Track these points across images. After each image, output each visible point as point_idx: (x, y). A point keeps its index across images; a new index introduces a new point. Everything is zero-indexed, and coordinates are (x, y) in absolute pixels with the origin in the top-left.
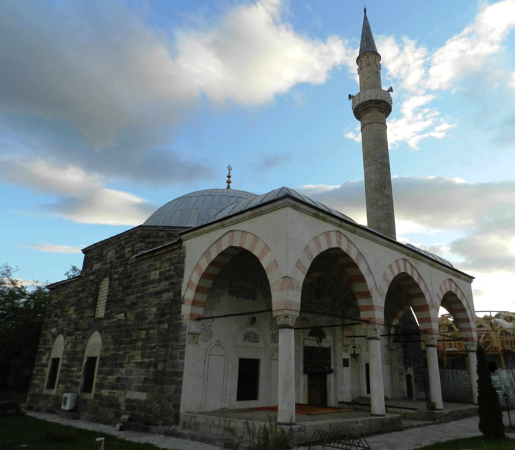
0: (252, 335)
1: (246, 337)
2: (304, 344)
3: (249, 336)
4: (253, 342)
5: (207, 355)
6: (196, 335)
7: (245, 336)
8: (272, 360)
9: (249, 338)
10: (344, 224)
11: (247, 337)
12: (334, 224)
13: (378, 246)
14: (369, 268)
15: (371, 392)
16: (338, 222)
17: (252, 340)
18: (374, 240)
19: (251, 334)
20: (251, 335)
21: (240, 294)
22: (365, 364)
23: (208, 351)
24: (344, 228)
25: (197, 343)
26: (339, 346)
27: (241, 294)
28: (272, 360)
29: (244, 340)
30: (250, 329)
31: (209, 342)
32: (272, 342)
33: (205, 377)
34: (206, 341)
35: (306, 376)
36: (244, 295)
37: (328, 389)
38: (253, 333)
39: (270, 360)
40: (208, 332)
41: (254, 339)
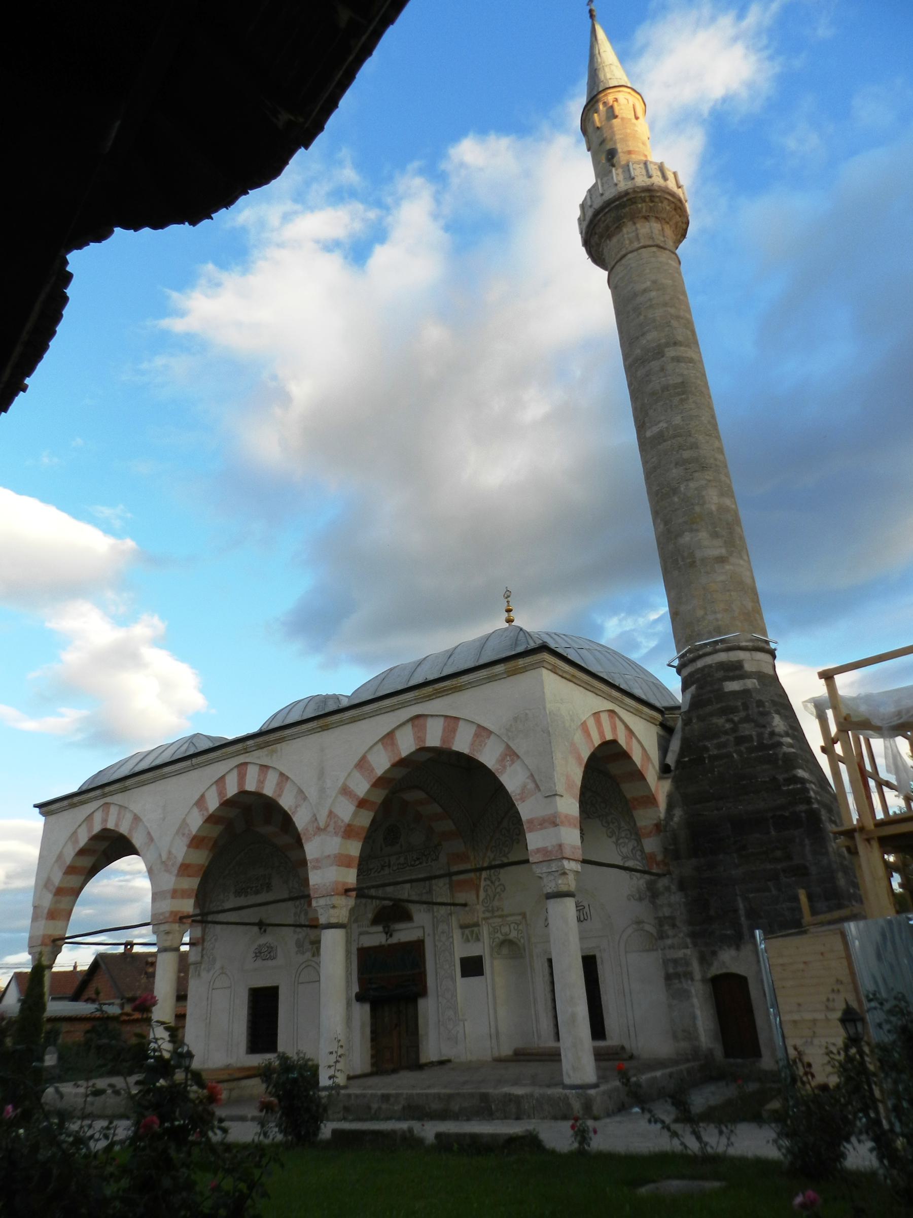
0: (266, 949)
1: (258, 955)
2: (358, 944)
3: (262, 951)
4: (267, 959)
5: (211, 989)
6: (198, 965)
7: (256, 953)
8: (299, 985)
9: (263, 954)
10: (107, 789)
11: (258, 954)
12: (96, 798)
13: (174, 780)
14: (149, 833)
15: (607, 1036)
16: (98, 792)
17: (266, 956)
18: (164, 777)
19: (265, 947)
20: (265, 948)
21: (249, 890)
22: (546, 960)
23: (212, 983)
24: (112, 794)
25: (199, 975)
26: (443, 932)
27: (251, 890)
28: (298, 984)
29: (255, 959)
30: (263, 940)
31: (211, 973)
32: (297, 954)
33: (208, 1021)
34: (208, 971)
35: (367, 1007)
36: (254, 889)
37: (421, 1031)
38: (268, 945)
39: (296, 983)
40: (211, 957)
41: (269, 955)
